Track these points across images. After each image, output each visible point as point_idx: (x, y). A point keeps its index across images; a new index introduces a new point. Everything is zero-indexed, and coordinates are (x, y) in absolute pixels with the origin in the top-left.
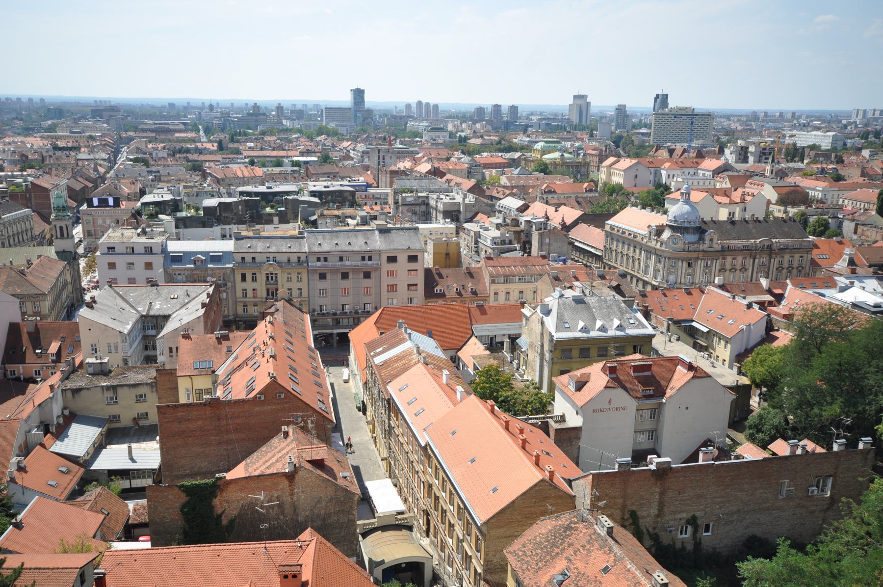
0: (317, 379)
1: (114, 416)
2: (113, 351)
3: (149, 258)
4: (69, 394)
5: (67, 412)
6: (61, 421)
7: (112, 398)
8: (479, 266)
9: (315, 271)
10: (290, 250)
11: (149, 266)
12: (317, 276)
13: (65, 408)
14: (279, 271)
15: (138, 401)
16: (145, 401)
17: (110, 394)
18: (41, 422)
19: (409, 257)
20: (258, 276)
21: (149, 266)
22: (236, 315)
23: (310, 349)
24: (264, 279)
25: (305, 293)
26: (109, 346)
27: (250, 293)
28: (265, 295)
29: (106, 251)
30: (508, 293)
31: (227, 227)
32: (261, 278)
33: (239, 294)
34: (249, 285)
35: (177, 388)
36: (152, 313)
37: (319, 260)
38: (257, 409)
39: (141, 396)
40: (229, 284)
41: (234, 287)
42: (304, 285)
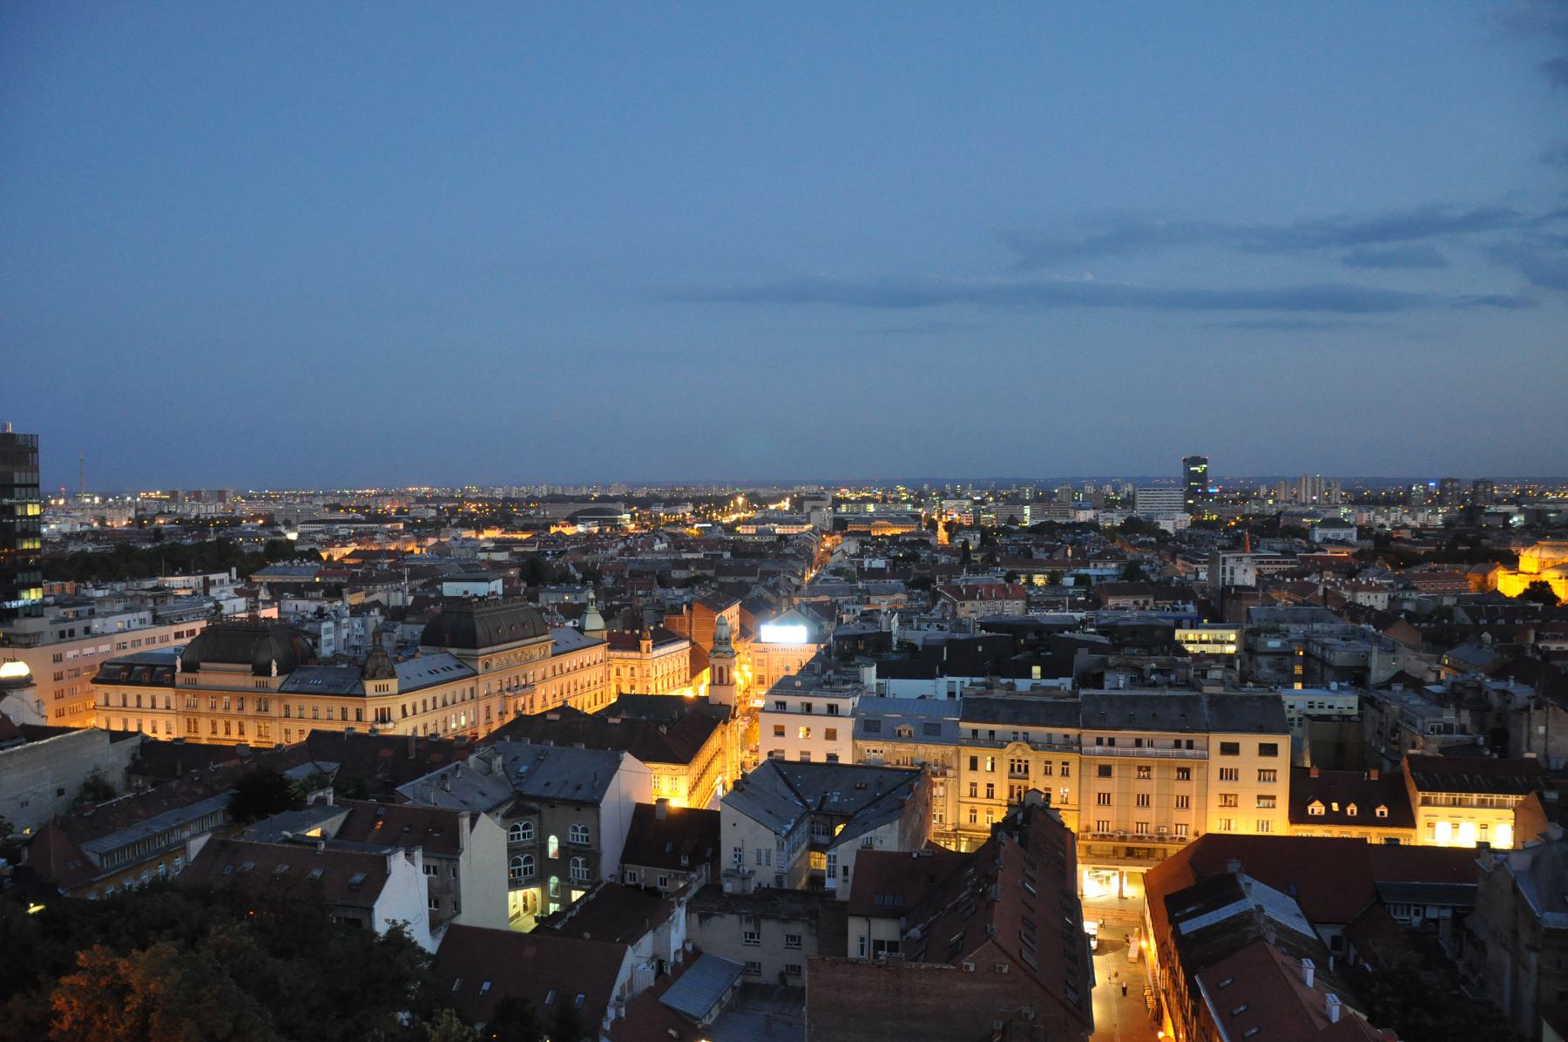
1: (753, 964)
2: (763, 859)
3: (831, 722)
5: (689, 947)
6: (680, 960)
7: (752, 936)
12: (1095, 770)
18: (654, 957)
19: (1261, 746)
24: (1007, 768)
26: (759, 853)
31: (958, 680)
35: (846, 933)
39: (793, 938)
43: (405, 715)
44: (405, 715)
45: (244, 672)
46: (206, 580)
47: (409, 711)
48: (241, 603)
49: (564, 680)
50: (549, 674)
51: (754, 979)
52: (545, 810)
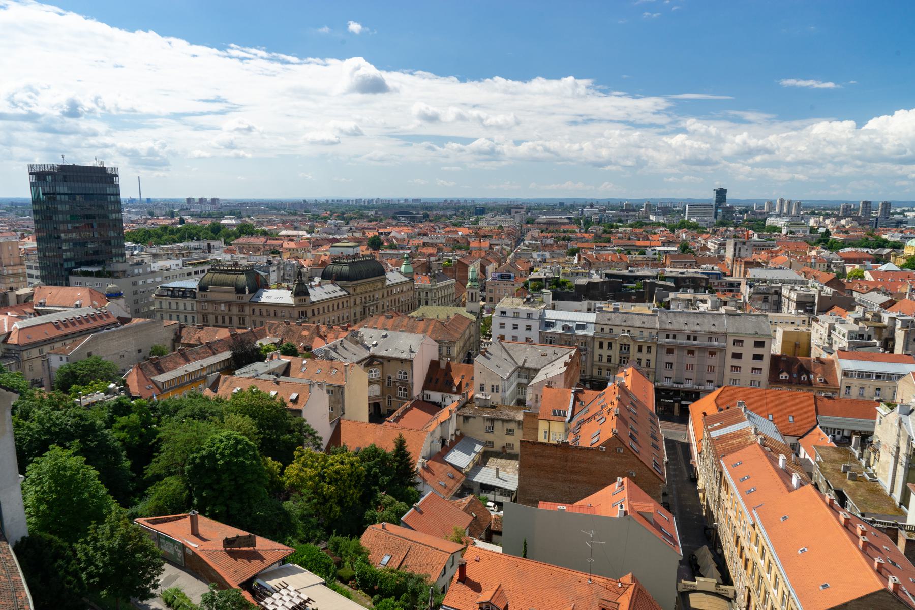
0: (655, 442)
3: (529, 322)
4: (461, 419)
5: (458, 433)
8: (830, 357)
9: (663, 346)
10: (643, 326)
11: (529, 328)
12: (665, 351)
13: (457, 429)
14: (632, 343)
15: (508, 434)
16: (513, 434)
17: (488, 424)
20: (613, 345)
21: (529, 328)
22: (592, 376)
23: (651, 414)
24: (618, 348)
25: (653, 364)
27: (605, 359)
28: (617, 362)
29: (499, 314)
30: (848, 387)
31: (593, 302)
32: (616, 347)
33: (596, 358)
34: (605, 352)
35: (537, 429)
36: (526, 365)
37: (668, 337)
38: (599, 458)
39: (510, 430)
40: (589, 350)
41: (593, 352)
42: (652, 357)
43: (314, 314)
44: (314, 314)
45: (232, 293)
46: (209, 245)
47: (316, 312)
48: (228, 257)
49: (393, 298)
50: (385, 295)
51: (490, 449)
52: (386, 363)
